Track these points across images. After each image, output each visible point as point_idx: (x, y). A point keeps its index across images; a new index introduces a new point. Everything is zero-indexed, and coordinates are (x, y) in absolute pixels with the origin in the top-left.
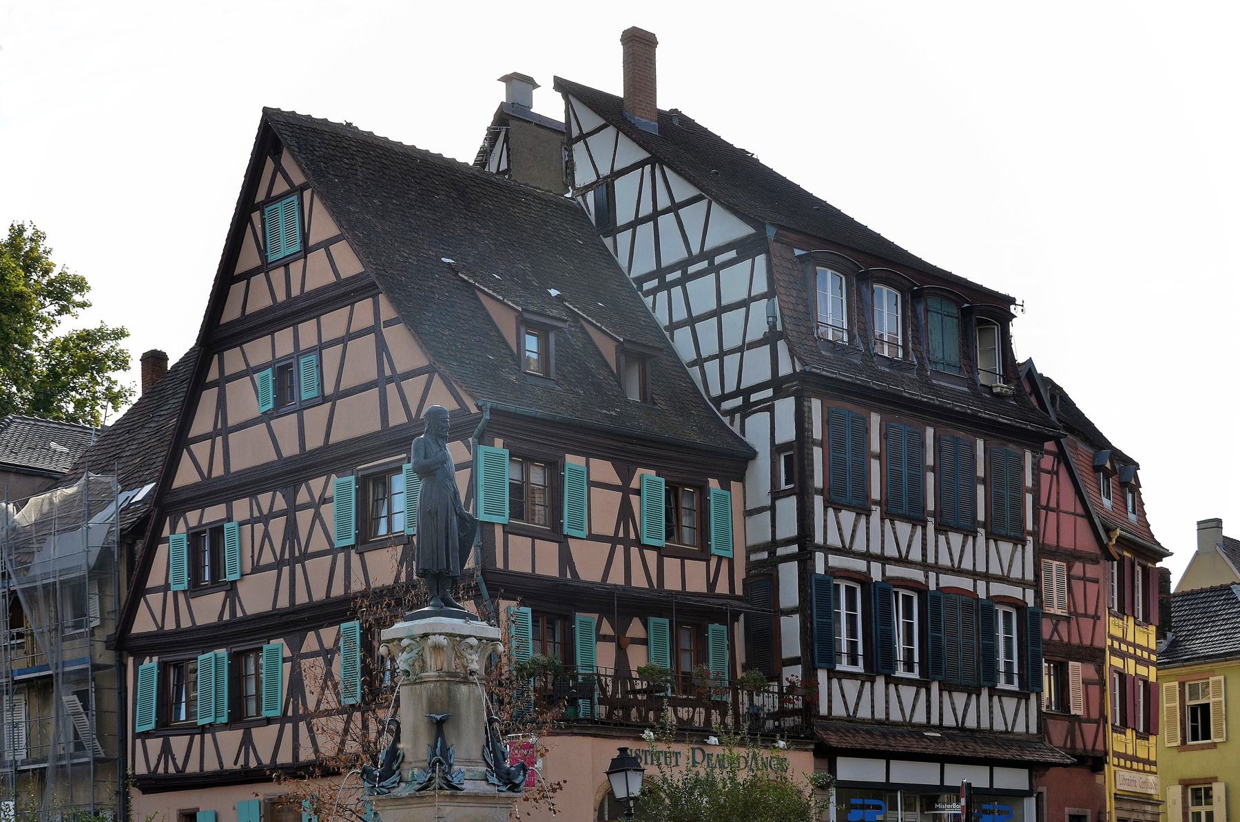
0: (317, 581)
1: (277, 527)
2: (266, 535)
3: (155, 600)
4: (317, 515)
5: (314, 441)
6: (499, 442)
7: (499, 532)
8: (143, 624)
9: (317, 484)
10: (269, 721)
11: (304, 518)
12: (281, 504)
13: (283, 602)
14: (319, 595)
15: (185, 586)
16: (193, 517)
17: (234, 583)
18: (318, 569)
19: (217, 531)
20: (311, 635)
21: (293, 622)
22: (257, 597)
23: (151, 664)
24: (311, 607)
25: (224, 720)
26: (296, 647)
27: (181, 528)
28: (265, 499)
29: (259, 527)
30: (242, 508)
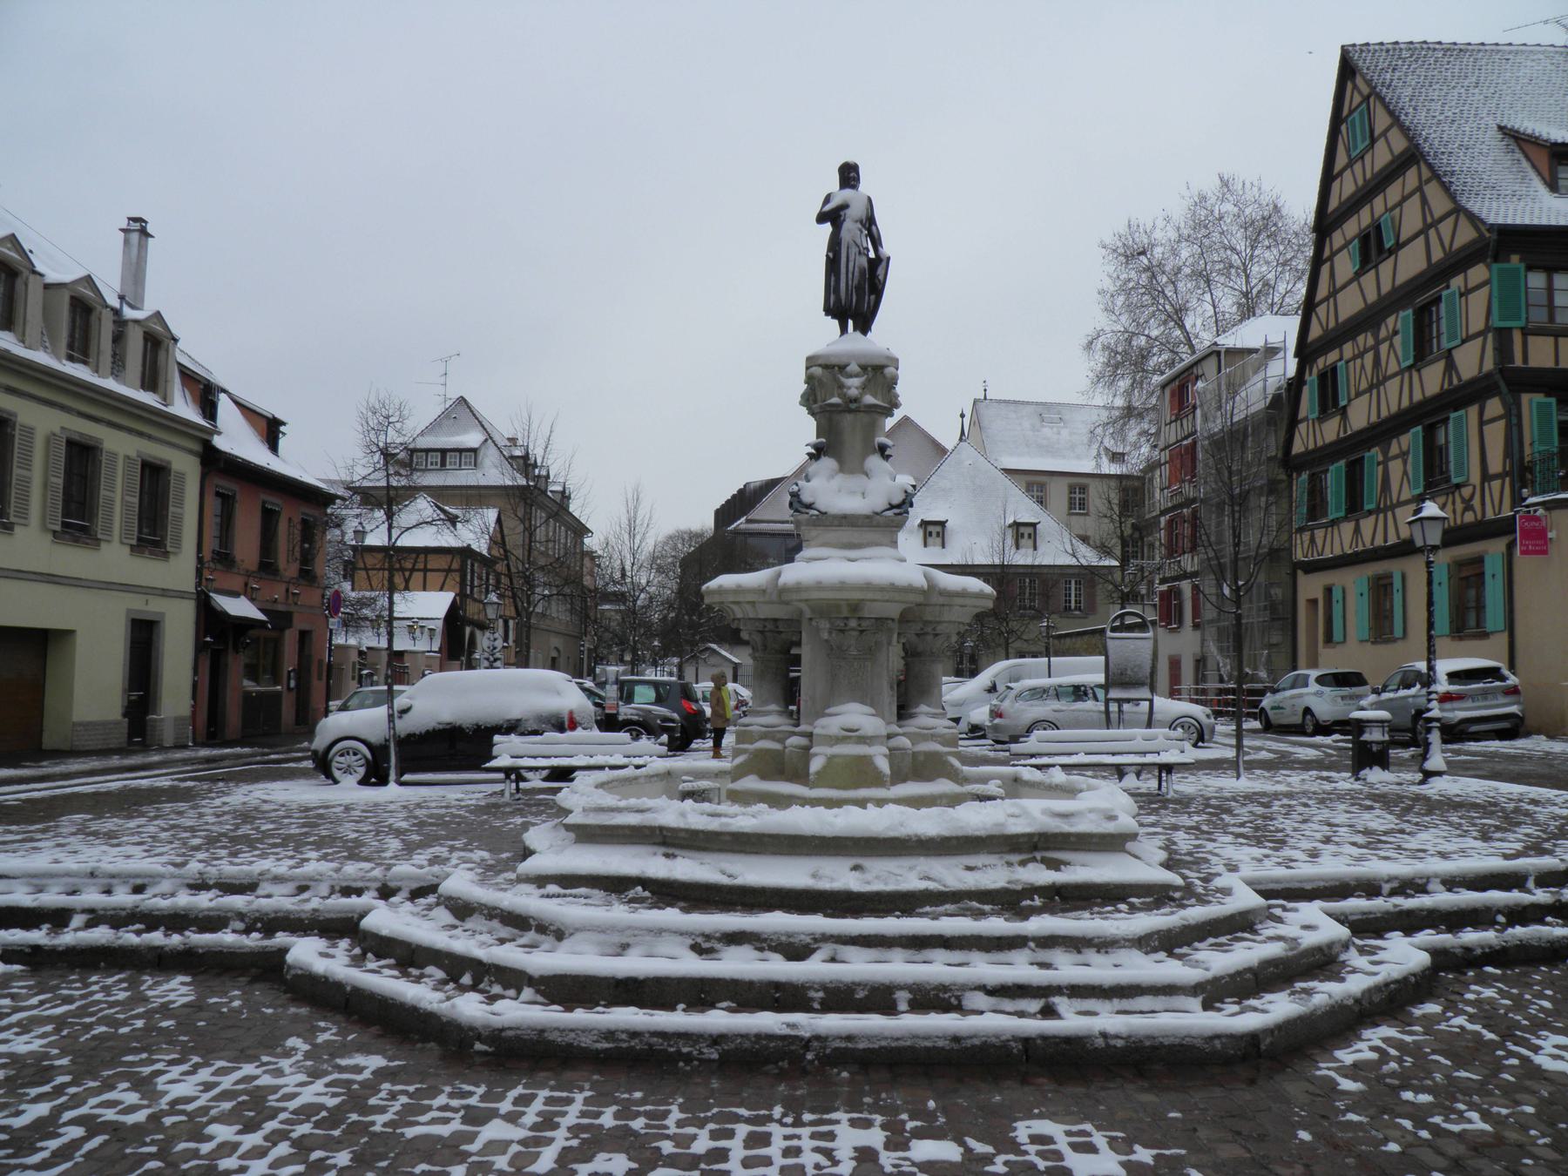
0: (1394, 398)
1: (1369, 357)
2: (1363, 367)
3: (1302, 427)
4: (1391, 345)
5: (1386, 287)
6: (1515, 258)
7: (1517, 337)
8: (1298, 448)
9: (1391, 321)
10: (1370, 513)
11: (1384, 348)
12: (1371, 341)
13: (1374, 418)
14: (1394, 409)
15: (1316, 415)
16: (1321, 363)
17: (1345, 407)
18: (1393, 386)
19: (1334, 369)
20: (1395, 441)
21: (1383, 431)
22: (1360, 415)
23: (1305, 476)
24: (1392, 418)
25: (1342, 514)
26: (1385, 453)
27: (1315, 370)
28: (1361, 339)
29: (1359, 361)
30: (1348, 349)
